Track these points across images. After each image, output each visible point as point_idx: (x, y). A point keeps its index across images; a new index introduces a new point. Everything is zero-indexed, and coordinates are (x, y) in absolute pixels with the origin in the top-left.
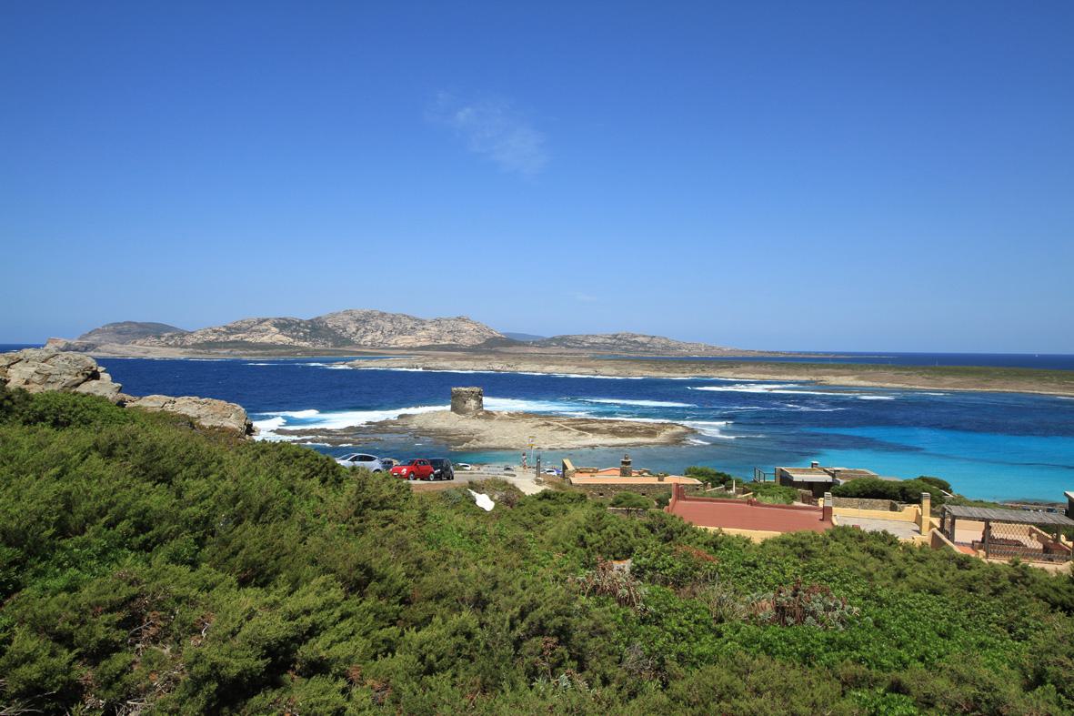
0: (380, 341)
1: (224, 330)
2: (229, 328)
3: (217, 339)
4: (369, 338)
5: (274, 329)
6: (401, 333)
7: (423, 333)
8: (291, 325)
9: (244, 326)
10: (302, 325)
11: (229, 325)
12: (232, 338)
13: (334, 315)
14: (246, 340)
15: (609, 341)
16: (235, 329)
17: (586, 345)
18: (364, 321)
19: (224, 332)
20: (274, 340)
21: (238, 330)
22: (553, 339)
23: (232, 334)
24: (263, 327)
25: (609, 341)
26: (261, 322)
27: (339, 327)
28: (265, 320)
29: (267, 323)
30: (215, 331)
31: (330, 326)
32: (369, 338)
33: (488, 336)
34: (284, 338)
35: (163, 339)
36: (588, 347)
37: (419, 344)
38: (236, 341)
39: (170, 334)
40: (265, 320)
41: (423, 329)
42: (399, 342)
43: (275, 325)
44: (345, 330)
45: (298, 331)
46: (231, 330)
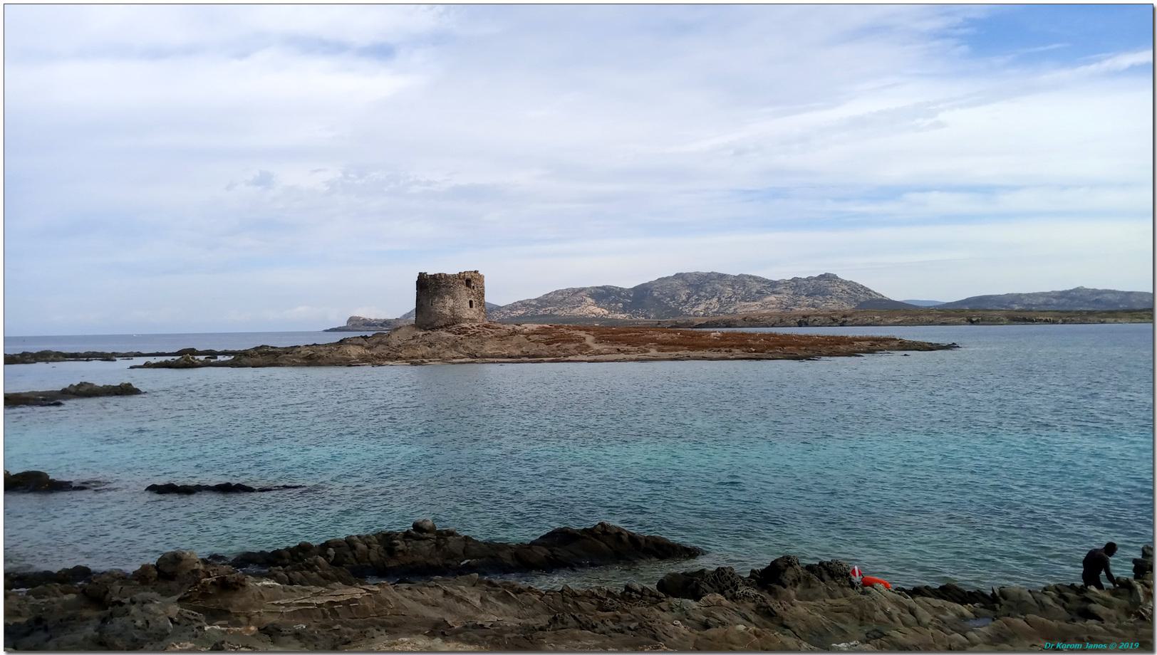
4: (702, 307)
5: (590, 300)
6: (744, 299)
7: (772, 298)
8: (610, 295)
12: (541, 312)
15: (1055, 301)
18: (698, 286)
20: (586, 312)
25: (1055, 301)
32: (702, 307)
33: (862, 298)
34: (598, 310)
41: (774, 293)
43: (592, 296)
44: (673, 298)
45: (617, 302)
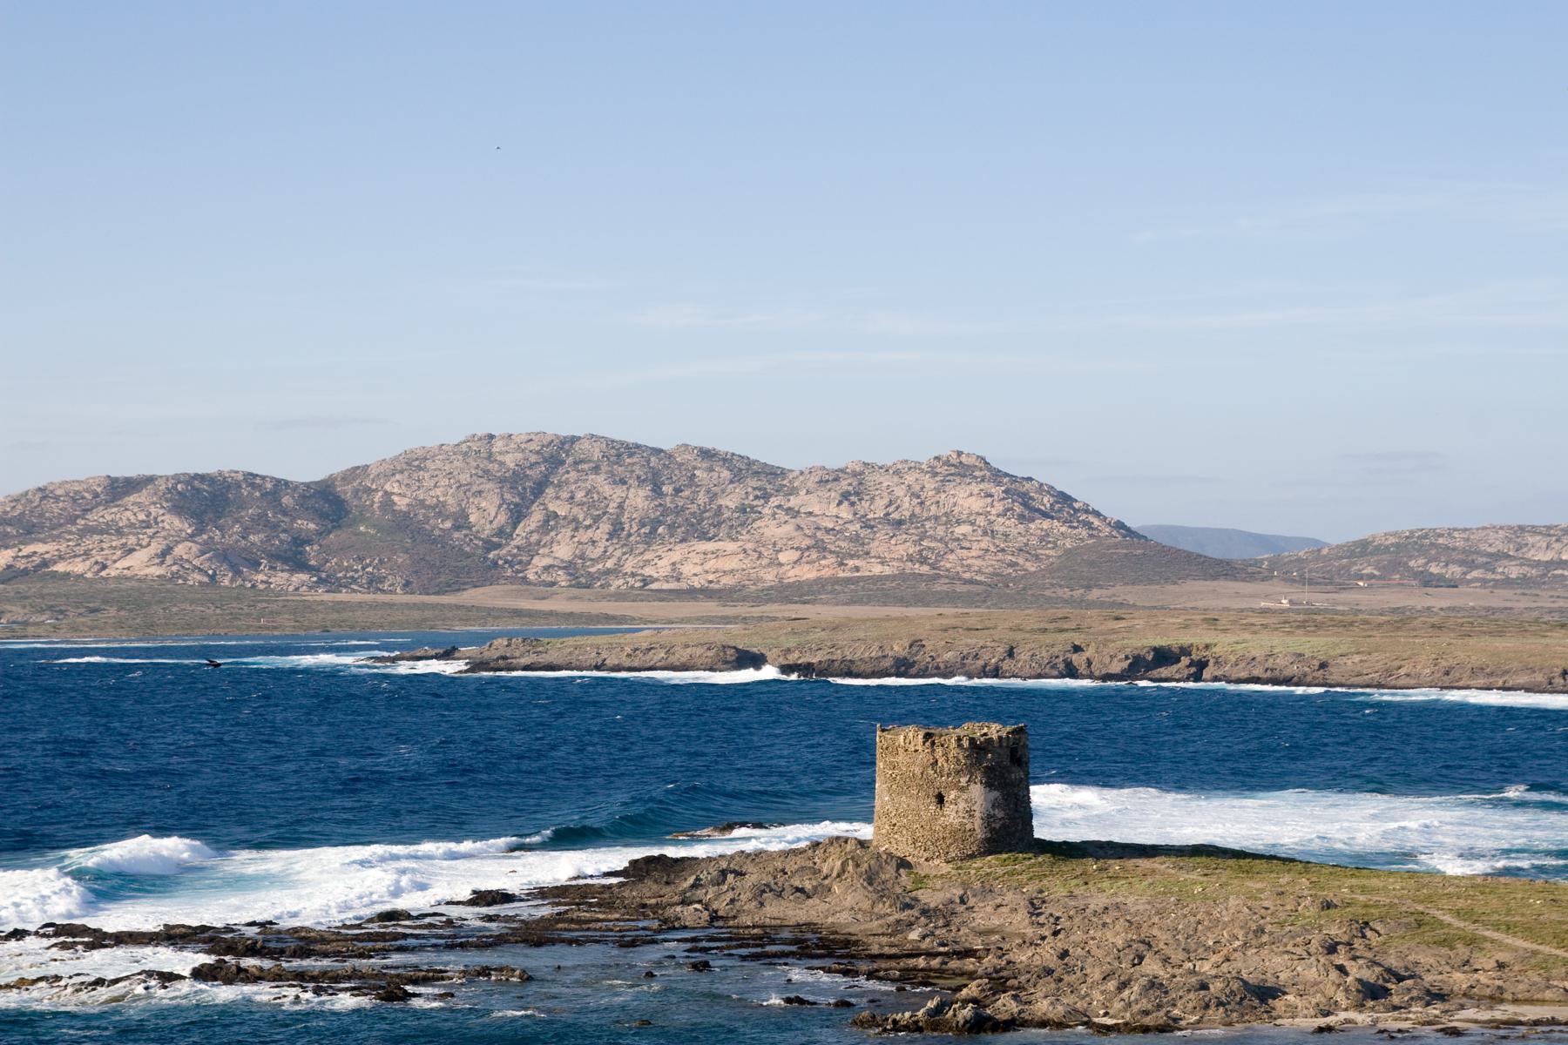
0: (610, 564)
5: (174, 523)
10: (286, 500)
13: (413, 464)
14: (60, 567)
17: (1514, 572)
22: (1363, 548)
26: (120, 489)
27: (439, 509)
29: (143, 497)
31: (401, 503)
36: (1524, 581)
37: (769, 576)
42: (687, 569)
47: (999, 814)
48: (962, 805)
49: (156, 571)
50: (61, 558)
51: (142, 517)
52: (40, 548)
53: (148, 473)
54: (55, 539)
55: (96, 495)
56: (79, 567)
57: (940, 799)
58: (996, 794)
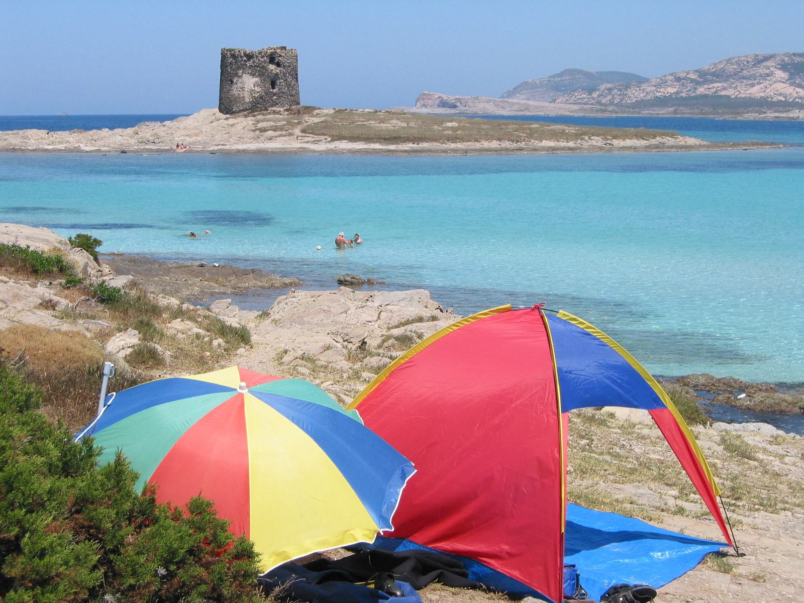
1: (692, 76)
2: (702, 74)
3: (677, 93)
5: (780, 74)
9: (731, 68)
11: (706, 68)
12: (701, 90)
14: (723, 93)
16: (713, 74)
19: (692, 81)
20: (770, 92)
21: (719, 75)
23: (706, 82)
24: (762, 71)
26: (759, 61)
28: (767, 58)
29: (768, 63)
30: (678, 79)
35: (595, 95)
38: (706, 96)
39: (609, 86)
40: (767, 58)
43: (784, 67)
46: (704, 77)
47: (257, 89)
48: (239, 85)
49: (762, 95)
50: (724, 89)
51: (767, 71)
52: (719, 84)
53: (772, 53)
54: (725, 81)
55: (748, 62)
56: (731, 93)
57: (232, 82)
58: (256, 79)
